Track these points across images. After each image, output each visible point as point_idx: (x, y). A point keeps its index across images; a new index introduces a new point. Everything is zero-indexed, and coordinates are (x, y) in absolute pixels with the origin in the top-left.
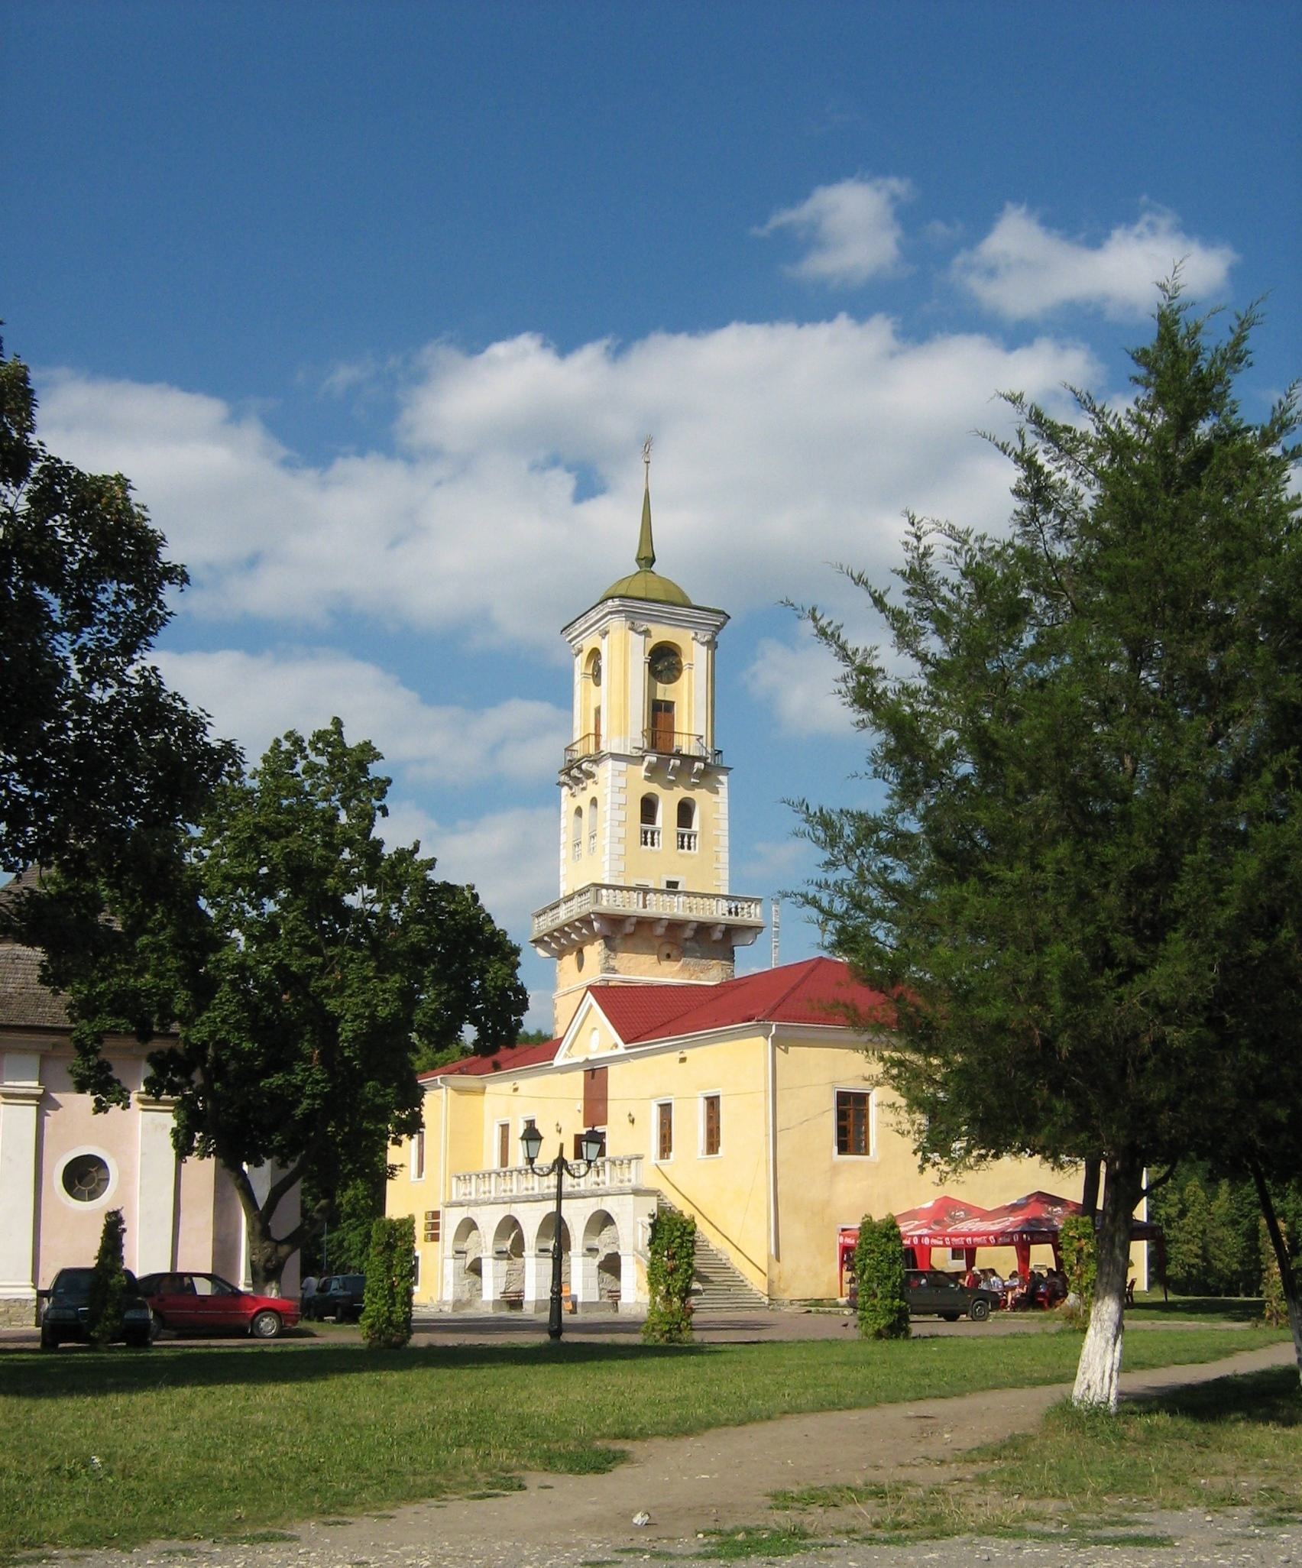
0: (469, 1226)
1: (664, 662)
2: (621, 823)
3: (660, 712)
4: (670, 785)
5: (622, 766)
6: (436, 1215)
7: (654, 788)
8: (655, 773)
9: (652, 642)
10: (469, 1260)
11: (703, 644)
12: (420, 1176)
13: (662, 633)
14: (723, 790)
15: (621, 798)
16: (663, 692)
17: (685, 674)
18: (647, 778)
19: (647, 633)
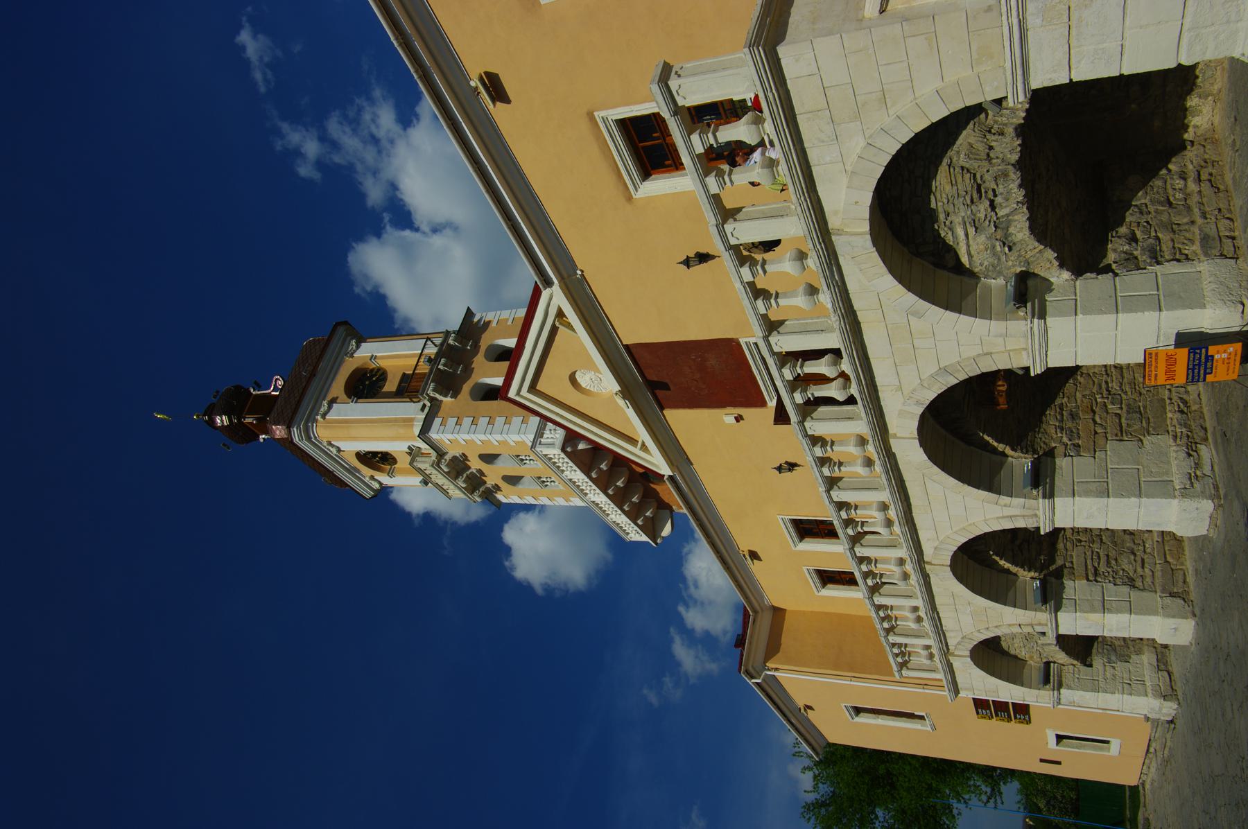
0: (991, 654)
1: (366, 385)
2: (491, 422)
3: (408, 388)
4: (468, 371)
5: (437, 421)
6: (980, 705)
7: (467, 388)
8: (449, 384)
9: (343, 396)
10: (1061, 657)
11: (358, 347)
12: (922, 718)
13: (338, 388)
14: (490, 316)
15: (467, 421)
16: (391, 386)
17: (383, 364)
18: (455, 396)
19: (333, 401)
